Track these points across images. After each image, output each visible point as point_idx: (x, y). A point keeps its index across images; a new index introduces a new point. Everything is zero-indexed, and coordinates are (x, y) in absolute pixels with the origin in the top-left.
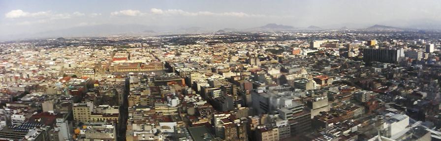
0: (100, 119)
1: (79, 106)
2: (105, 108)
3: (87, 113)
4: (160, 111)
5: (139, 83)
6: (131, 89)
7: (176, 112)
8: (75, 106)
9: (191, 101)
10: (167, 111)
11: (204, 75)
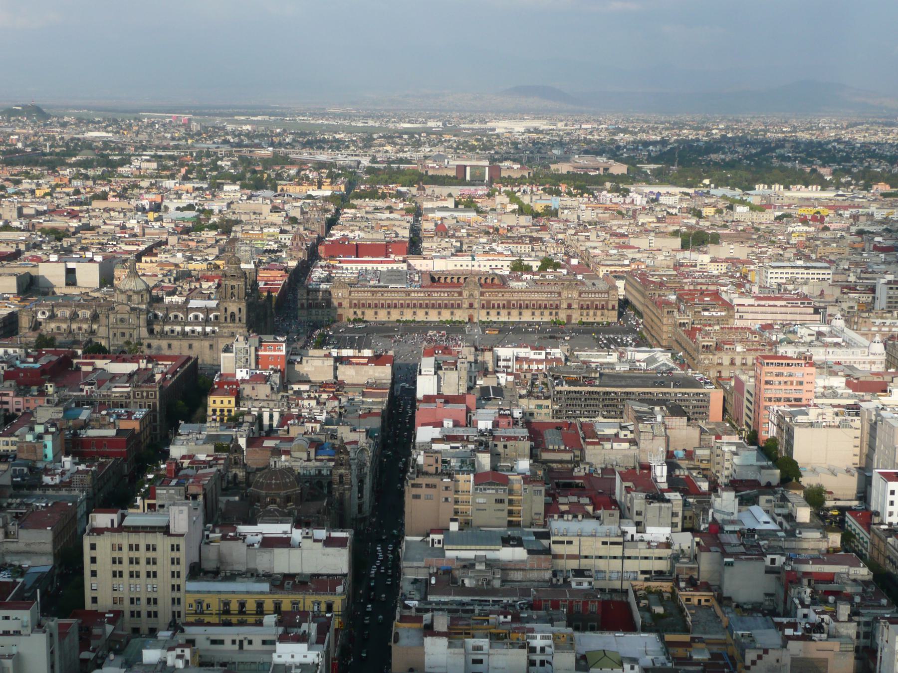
0: (234, 607)
1: (121, 529)
2: (269, 543)
3: (164, 568)
4: (573, 564)
6: (424, 434)
7: (660, 575)
8: (99, 531)
9: (749, 524)
10: (616, 565)
11: (838, 382)
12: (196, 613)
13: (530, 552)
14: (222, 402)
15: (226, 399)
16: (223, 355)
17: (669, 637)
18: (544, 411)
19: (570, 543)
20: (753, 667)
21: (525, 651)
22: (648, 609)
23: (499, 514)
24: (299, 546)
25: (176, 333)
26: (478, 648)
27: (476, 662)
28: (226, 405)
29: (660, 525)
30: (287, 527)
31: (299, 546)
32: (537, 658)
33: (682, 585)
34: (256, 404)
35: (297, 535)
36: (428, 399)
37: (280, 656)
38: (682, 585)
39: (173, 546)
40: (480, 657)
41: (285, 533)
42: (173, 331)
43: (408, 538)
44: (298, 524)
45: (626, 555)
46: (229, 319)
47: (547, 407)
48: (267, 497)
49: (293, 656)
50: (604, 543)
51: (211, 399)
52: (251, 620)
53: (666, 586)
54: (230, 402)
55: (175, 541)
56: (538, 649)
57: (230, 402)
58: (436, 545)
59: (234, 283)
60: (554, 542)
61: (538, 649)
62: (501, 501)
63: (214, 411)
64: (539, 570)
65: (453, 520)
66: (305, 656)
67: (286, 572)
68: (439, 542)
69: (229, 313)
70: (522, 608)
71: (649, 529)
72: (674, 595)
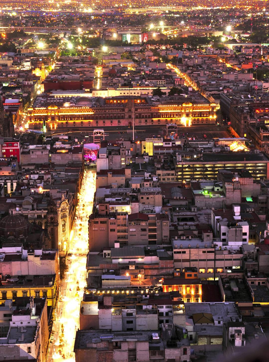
4: (187, 264)
13: (161, 258)
17: (241, 304)
18: (171, 177)
19: (184, 252)
21: (156, 316)
22: (229, 289)
23: (143, 237)
26: (130, 314)
27: (129, 322)
30: (19, 249)
32: (164, 319)
33: (249, 274)
37: (14, 323)
38: (249, 274)
40: (131, 319)
41: (18, 252)
48: (8, 232)
49: (22, 323)
50: (204, 252)
56: (164, 314)
58: (107, 257)
61: (164, 314)
62: (144, 230)
64: (166, 268)
65: (117, 242)
68: (109, 255)
71: (230, 243)
72: (244, 282)
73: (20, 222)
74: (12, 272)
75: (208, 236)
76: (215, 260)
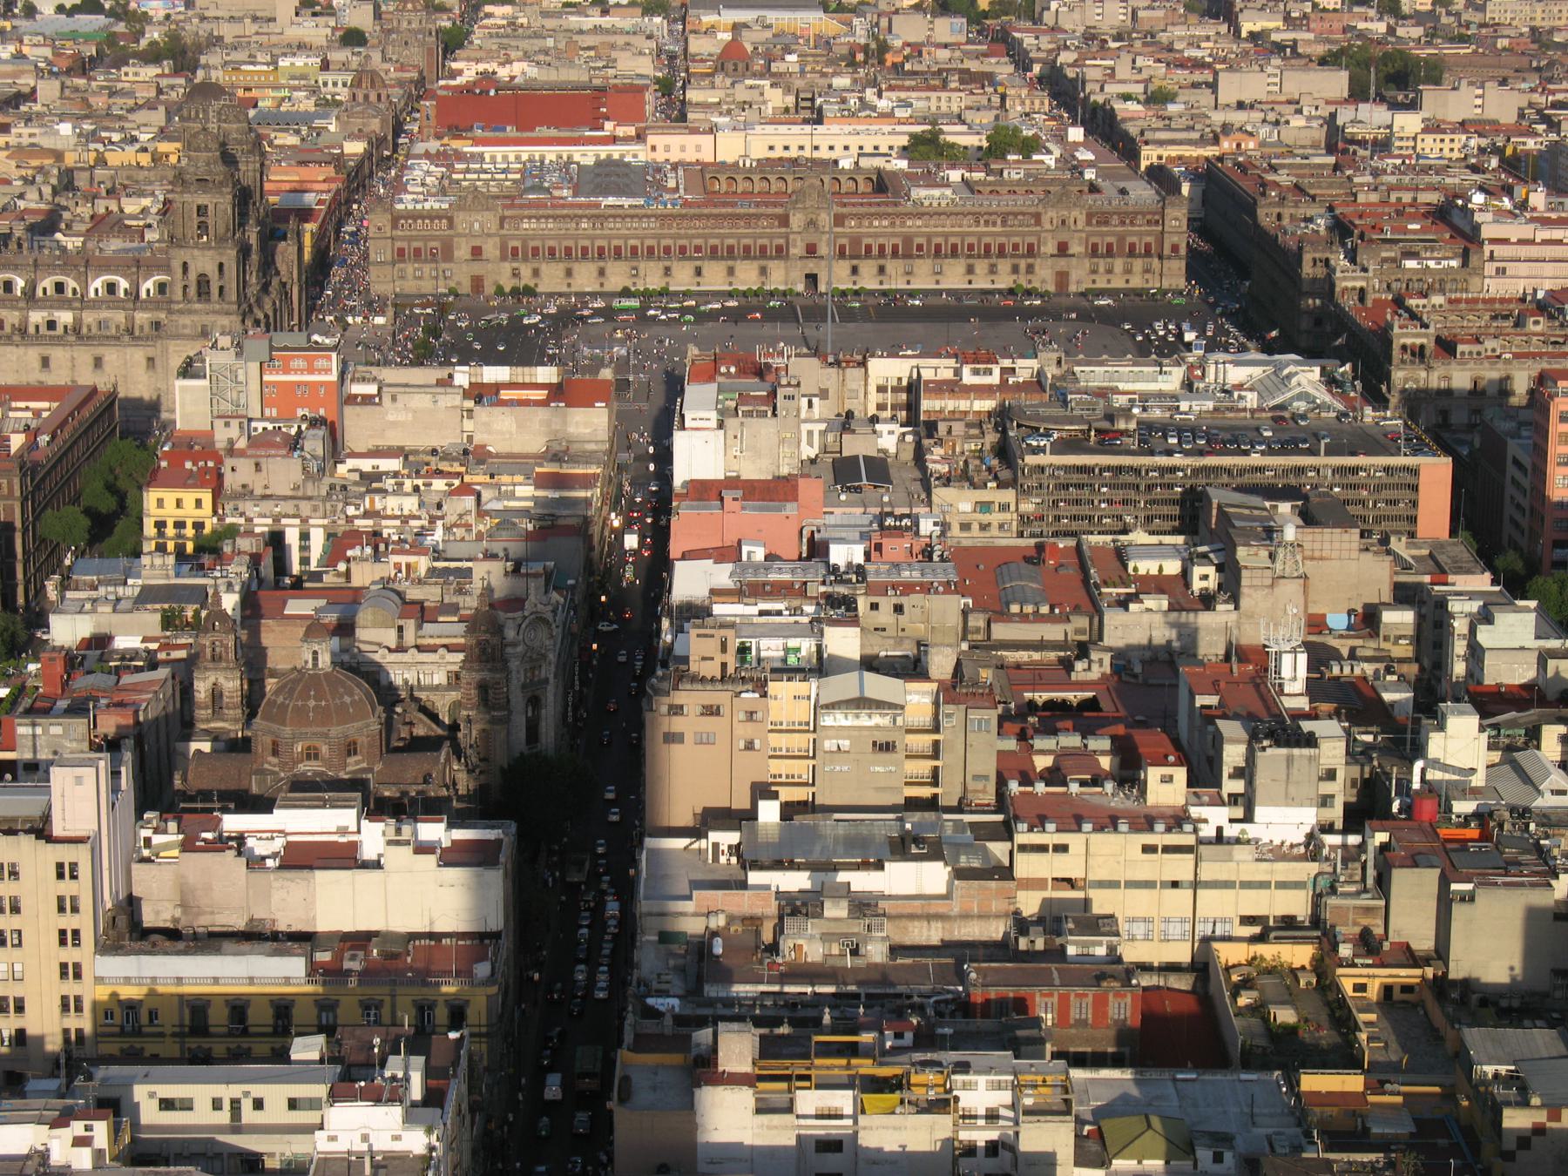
5: (810, 490)
12: (122, 1033)
14: (179, 504)
15: (189, 497)
16: (180, 383)
18: (995, 518)
19: (1062, 848)
20: (1522, 1155)
24: (376, 865)
25: (60, 330)
28: (189, 513)
29: (1290, 800)
31: (376, 865)
34: (267, 506)
35: (373, 837)
36: (704, 491)
37: (333, 1139)
38: (1345, 951)
39: (60, 866)
41: (343, 831)
42: (51, 325)
43: (650, 842)
44: (376, 808)
45: (1205, 875)
46: (192, 291)
47: (1004, 508)
50: (1148, 849)
51: (151, 497)
52: (262, 1048)
53: (1300, 955)
54: (199, 503)
55: (66, 854)
57: (199, 503)
59: (203, 199)
60: (1023, 848)
63: (160, 525)
66: (397, 1138)
67: (348, 927)
69: (193, 276)
70: (940, 1014)
73: (347, 699)
74: (314, 918)
75: (1168, 779)
76: (1196, 885)
